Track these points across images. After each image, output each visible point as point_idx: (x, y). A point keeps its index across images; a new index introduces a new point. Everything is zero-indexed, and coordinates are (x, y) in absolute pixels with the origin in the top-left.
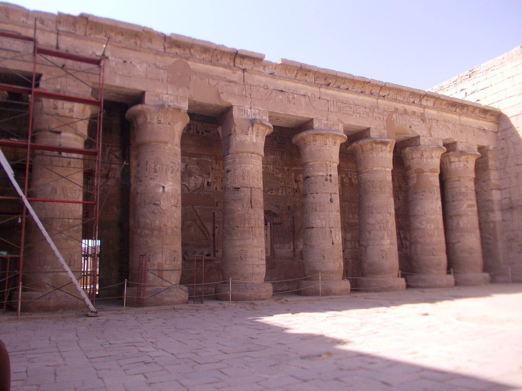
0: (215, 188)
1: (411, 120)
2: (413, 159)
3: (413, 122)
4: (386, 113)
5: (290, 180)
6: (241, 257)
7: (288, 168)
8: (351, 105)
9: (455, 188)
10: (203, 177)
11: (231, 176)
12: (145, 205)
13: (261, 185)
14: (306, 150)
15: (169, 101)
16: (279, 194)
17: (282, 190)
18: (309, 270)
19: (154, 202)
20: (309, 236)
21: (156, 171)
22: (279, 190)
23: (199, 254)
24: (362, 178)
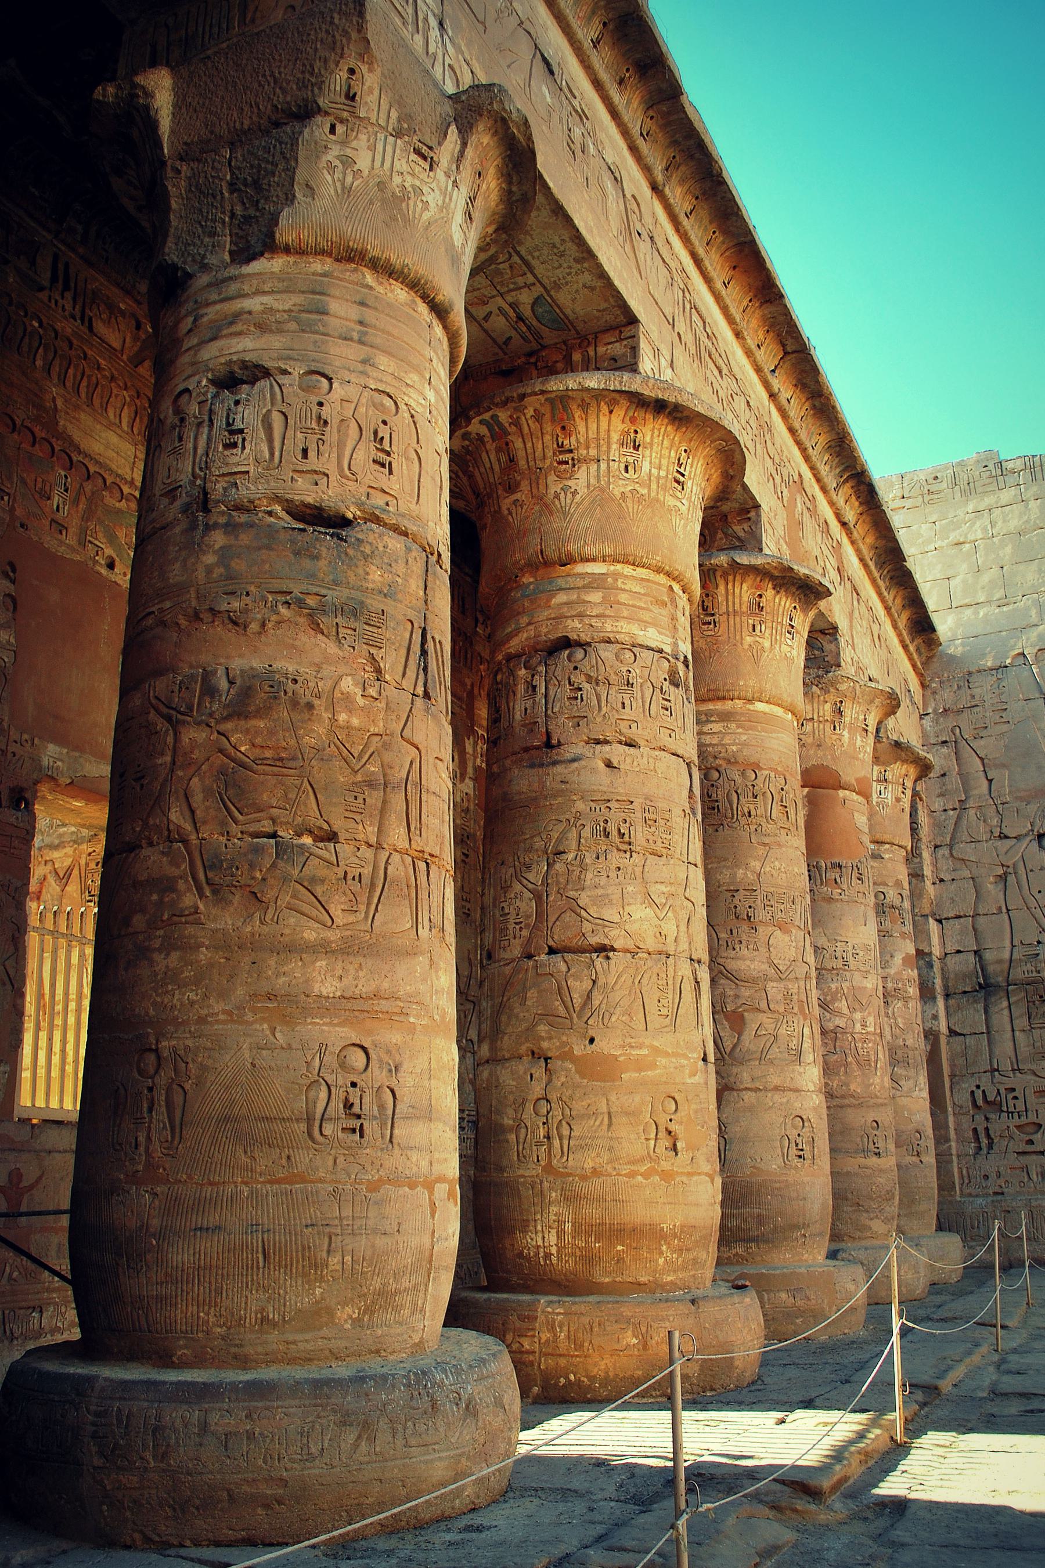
6: (348, 1105)
11: (277, 420)
20: (578, 1001)
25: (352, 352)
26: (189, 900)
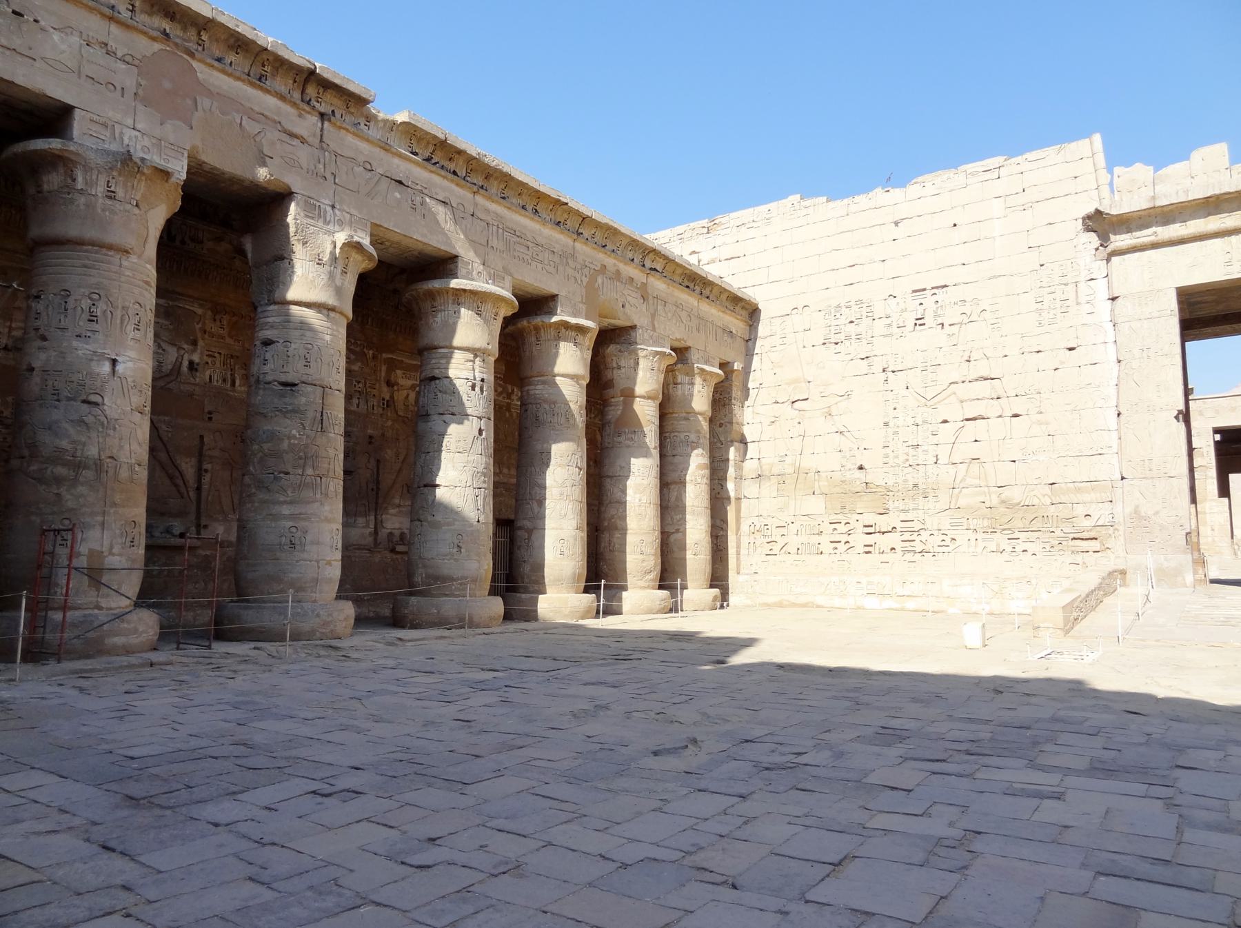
0: (208, 378)
1: (626, 292)
2: (619, 368)
3: (629, 298)
4: (586, 271)
5: (377, 380)
6: (291, 541)
7: (373, 354)
8: (529, 243)
9: (679, 432)
10: (180, 348)
11: (275, 356)
12: (58, 400)
13: (342, 386)
14: (434, 321)
15: (139, 147)
16: (352, 409)
17: (359, 398)
18: (424, 575)
19: (85, 397)
21: (95, 319)
22: (351, 399)
23: (162, 533)
24: (532, 392)
25: (297, 333)
26: (253, 490)
